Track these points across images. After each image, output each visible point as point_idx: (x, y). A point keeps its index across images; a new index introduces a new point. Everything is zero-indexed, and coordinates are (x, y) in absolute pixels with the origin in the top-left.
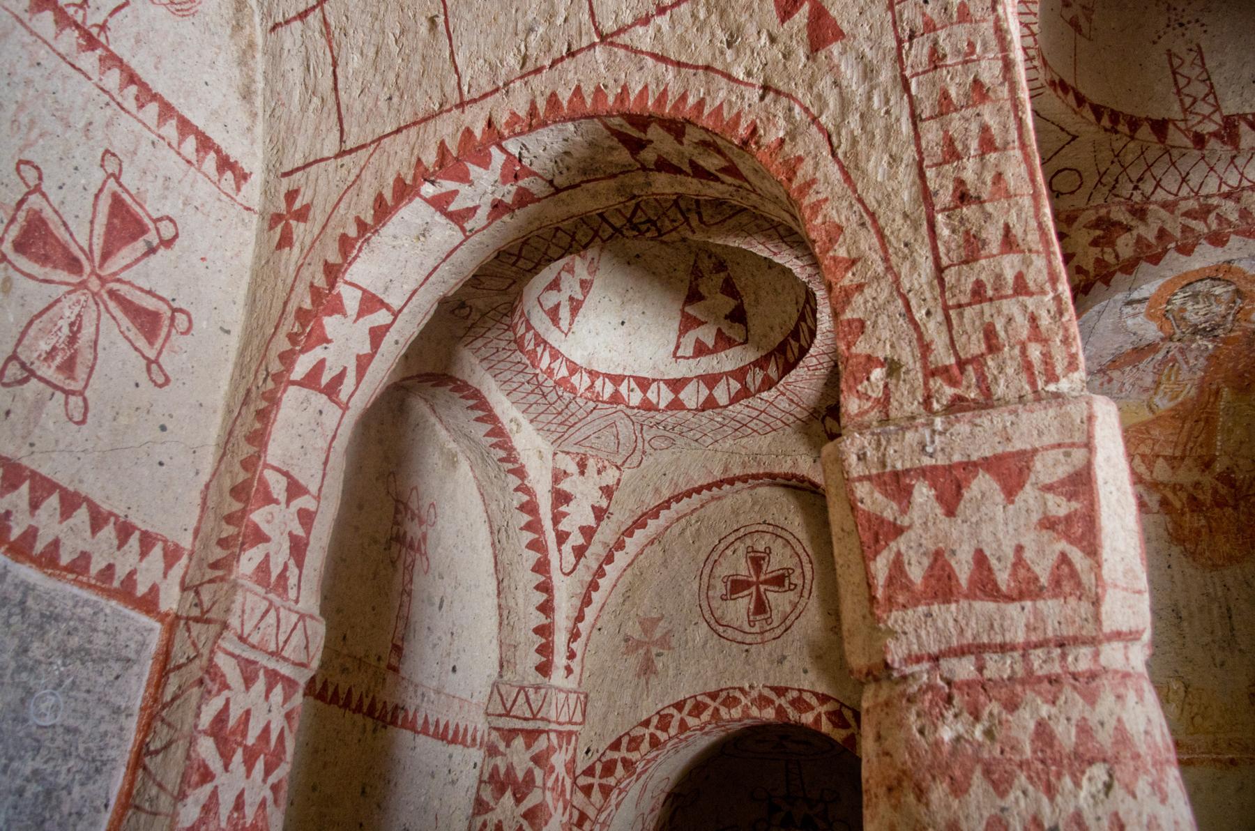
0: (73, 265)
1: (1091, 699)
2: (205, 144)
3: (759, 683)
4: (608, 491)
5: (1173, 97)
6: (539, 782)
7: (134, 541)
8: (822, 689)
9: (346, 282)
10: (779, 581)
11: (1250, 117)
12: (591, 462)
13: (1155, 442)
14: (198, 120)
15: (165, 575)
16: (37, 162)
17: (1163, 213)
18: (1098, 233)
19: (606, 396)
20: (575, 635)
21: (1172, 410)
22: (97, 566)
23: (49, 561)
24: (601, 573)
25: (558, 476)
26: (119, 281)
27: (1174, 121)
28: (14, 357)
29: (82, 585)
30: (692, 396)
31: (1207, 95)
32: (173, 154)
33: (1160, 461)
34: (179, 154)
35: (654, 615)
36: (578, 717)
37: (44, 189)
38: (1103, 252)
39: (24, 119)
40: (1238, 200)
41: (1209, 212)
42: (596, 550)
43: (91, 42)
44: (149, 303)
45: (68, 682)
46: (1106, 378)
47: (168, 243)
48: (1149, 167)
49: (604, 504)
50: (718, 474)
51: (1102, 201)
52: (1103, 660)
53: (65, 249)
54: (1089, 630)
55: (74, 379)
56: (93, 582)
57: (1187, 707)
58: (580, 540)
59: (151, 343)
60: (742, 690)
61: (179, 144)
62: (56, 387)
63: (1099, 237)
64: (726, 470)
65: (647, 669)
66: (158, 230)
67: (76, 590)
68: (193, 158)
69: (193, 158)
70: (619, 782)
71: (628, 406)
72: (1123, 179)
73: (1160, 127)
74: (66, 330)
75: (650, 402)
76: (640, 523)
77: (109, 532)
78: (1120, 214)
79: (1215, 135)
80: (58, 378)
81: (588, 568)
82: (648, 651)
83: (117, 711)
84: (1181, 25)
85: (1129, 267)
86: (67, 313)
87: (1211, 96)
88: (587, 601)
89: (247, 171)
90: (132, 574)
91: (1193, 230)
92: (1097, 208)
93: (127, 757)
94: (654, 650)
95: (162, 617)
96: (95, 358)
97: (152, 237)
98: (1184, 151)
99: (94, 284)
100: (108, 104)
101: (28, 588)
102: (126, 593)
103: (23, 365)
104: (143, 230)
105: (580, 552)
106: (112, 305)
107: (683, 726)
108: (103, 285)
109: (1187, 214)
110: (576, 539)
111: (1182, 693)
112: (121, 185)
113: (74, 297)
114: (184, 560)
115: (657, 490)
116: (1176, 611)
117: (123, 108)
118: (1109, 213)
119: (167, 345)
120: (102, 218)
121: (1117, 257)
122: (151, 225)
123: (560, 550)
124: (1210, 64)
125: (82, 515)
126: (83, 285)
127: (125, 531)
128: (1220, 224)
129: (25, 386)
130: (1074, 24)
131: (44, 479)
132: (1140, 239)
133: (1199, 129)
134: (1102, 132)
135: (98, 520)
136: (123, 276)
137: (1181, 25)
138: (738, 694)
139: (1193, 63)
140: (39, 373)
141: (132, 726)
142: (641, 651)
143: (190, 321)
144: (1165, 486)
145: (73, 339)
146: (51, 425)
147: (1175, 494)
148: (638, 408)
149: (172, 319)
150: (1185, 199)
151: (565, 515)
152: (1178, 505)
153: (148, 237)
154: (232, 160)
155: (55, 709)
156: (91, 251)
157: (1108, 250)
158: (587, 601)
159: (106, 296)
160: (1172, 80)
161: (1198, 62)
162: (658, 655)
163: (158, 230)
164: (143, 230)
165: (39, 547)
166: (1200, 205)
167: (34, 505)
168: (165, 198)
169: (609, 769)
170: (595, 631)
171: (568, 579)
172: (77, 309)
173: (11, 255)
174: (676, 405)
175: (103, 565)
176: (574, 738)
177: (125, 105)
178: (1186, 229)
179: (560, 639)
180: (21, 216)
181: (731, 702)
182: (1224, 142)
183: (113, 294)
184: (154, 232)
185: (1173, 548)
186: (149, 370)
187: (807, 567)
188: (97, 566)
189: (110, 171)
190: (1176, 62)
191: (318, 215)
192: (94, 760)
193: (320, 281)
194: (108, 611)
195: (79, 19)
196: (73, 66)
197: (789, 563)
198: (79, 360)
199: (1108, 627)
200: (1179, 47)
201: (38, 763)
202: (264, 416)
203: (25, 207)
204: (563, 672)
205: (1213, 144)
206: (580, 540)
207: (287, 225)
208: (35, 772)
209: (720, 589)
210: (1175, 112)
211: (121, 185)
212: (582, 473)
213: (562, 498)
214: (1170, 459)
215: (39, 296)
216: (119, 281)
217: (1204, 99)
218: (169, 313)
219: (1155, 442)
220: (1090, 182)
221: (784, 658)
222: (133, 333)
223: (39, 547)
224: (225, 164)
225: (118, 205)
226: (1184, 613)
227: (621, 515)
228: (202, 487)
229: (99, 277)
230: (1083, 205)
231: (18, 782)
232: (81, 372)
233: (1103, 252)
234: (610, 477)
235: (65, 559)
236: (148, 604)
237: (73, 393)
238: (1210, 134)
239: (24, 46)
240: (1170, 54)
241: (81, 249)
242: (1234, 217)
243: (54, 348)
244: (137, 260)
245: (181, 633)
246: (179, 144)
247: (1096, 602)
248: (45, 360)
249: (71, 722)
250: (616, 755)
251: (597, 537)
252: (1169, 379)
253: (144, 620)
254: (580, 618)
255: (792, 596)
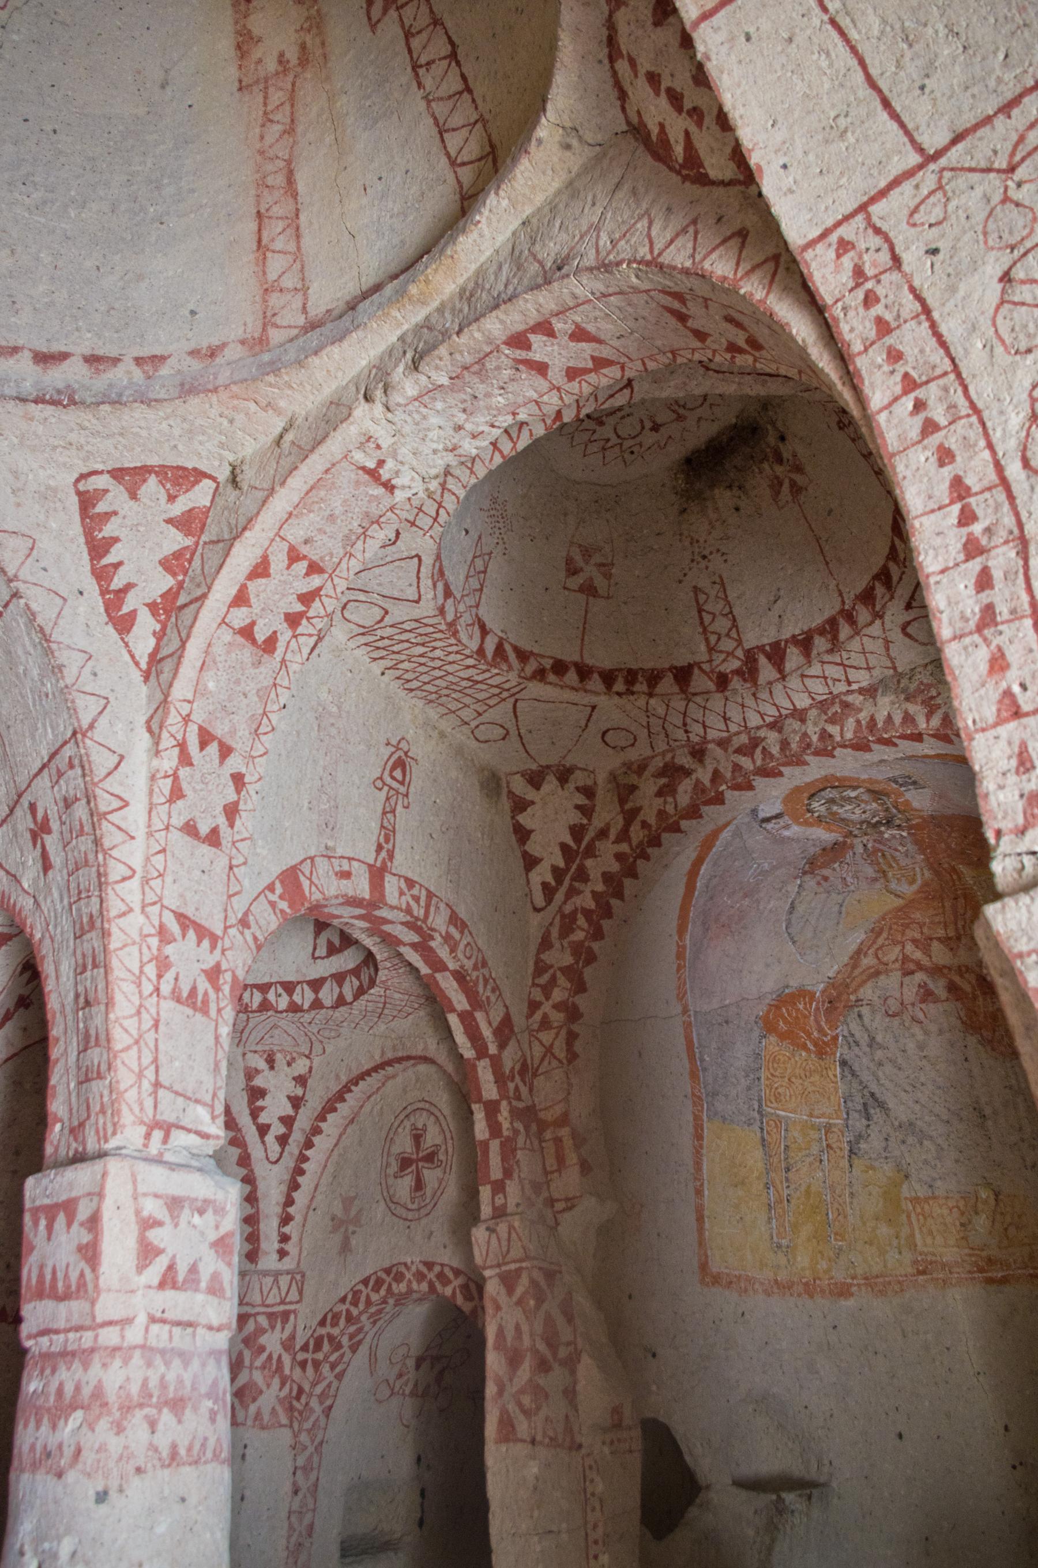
1: (86, 1365)
3: (414, 1259)
4: (301, 1080)
5: (699, 639)
6: (247, 1363)
8: (455, 1264)
10: (430, 1158)
11: (767, 648)
12: (279, 1056)
13: (921, 926)
17: (719, 751)
18: (663, 781)
19: (255, 1005)
20: (286, 1219)
21: (919, 891)
24: (303, 1158)
25: (250, 1074)
27: (698, 664)
30: (328, 994)
31: (730, 630)
33: (935, 944)
35: (353, 1194)
36: (294, 1295)
38: (665, 802)
40: (780, 731)
41: (756, 746)
42: (297, 1137)
46: (819, 878)
48: (685, 714)
49: (299, 1092)
50: (378, 1059)
51: (665, 747)
52: (100, 1339)
54: (88, 1323)
57: (998, 1217)
58: (282, 1130)
60: (405, 1264)
63: (664, 785)
64: (383, 1053)
65: (345, 1247)
70: (326, 1357)
71: (277, 1012)
72: (670, 728)
73: (683, 675)
75: (296, 1004)
76: (329, 1107)
78: (684, 760)
79: (738, 672)
81: (291, 1154)
82: (346, 1230)
84: (704, 557)
85: (693, 812)
87: (734, 630)
88: (294, 1186)
91: (741, 768)
92: (663, 754)
94: (351, 1228)
98: (706, 696)
105: (283, 1140)
107: (369, 1303)
109: (738, 751)
110: (278, 1129)
111: (992, 1202)
115: (337, 1077)
116: (978, 1109)
118: (673, 758)
121: (676, 806)
123: (263, 1142)
124: (732, 595)
128: (763, 759)
130: (589, 590)
132: (698, 782)
133: (722, 668)
134: (616, 697)
137: (704, 557)
138: (403, 1269)
139: (717, 597)
142: (343, 1230)
144: (950, 969)
147: (961, 976)
148: (286, 1011)
150: (738, 733)
151: (262, 1109)
152: (968, 988)
157: (670, 799)
158: (294, 1186)
160: (697, 621)
161: (721, 595)
162: (354, 1233)
166: (750, 739)
169: (318, 1346)
170: (311, 1212)
171: (276, 1168)
174: (317, 1004)
176: (292, 1317)
178: (737, 767)
179: (269, 1227)
181: (399, 1278)
182: (745, 680)
185: (969, 1038)
187: (450, 1145)
190: (702, 598)
197: (438, 1140)
199: (99, 1320)
200: (704, 583)
204: (275, 1256)
205: (736, 683)
206: (282, 1130)
209: (394, 1167)
210: (701, 653)
212: (272, 1068)
213: (256, 1094)
214: (945, 941)
217: (728, 635)
219: (921, 926)
220: (643, 734)
221: (431, 1233)
226: (988, 1111)
227: (314, 1103)
230: (649, 752)
233: (665, 802)
234: (301, 1067)
238: (732, 672)
240: (696, 590)
242: (775, 750)
247: (93, 1303)
250: (323, 1331)
251: (297, 1125)
252: (891, 866)
254: (289, 1202)
255: (438, 1172)
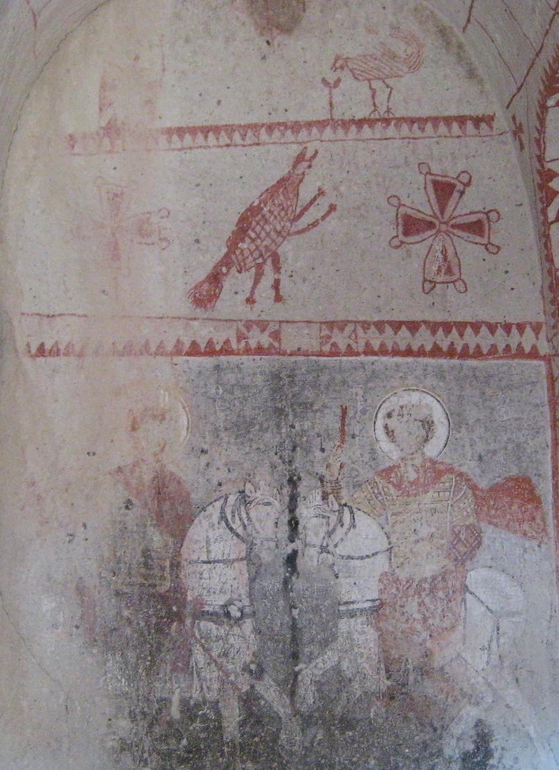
0: (431, 225)
2: (462, 120)
7: (514, 330)
9: (548, 162)
14: (453, 111)
15: (537, 339)
16: (394, 193)
22: (501, 347)
23: (478, 354)
26: (454, 218)
28: (425, 280)
29: (498, 358)
32: (449, 140)
34: (452, 137)
37: (403, 203)
39: (380, 180)
43: (387, 121)
44: (473, 218)
45: (507, 400)
47: (468, 184)
53: (423, 221)
55: (454, 274)
56: (502, 355)
59: (482, 236)
61: (450, 132)
62: (447, 283)
66: (459, 181)
67: (496, 362)
68: (460, 133)
69: (460, 133)
74: (441, 256)
77: (500, 331)
80: (448, 278)
83: (537, 405)
86: (437, 248)
89: (492, 114)
90: (519, 345)
93: (549, 423)
95: (544, 358)
96: (459, 260)
97: (460, 187)
99: (444, 227)
100: (409, 143)
101: (475, 369)
102: (520, 353)
103: (430, 282)
104: (452, 186)
106: (455, 231)
108: (448, 226)
112: (433, 175)
113: (437, 239)
114: (544, 328)
117: (416, 139)
119: (491, 231)
120: (432, 196)
122: (456, 182)
125: (484, 329)
126: (439, 231)
127: (507, 328)
129: (435, 289)
131: (459, 322)
135: (492, 328)
136: (456, 214)
140: (438, 281)
141: (547, 409)
143: (498, 213)
145: (445, 258)
146: (453, 299)
149: (488, 218)
153: (457, 188)
154: (480, 116)
155: (506, 412)
156: (435, 214)
159: (451, 230)
163: (459, 181)
164: (452, 186)
165: (471, 351)
167: (461, 335)
168: (456, 163)
172: (441, 244)
173: (405, 239)
175: (504, 346)
177: (416, 136)
180: (400, 220)
183: (453, 226)
184: (459, 184)
186: (487, 249)
188: (501, 347)
189: (425, 172)
191: (525, 128)
192: (533, 428)
193: (537, 165)
194: (515, 365)
195: (377, 117)
196: (386, 139)
198: (452, 265)
201: (509, 435)
202: (546, 245)
203: (399, 216)
207: (519, 136)
208: (509, 439)
211: (433, 175)
215: (421, 249)
216: (454, 218)
218: (485, 216)
222: (473, 237)
223: (471, 351)
224: (477, 121)
225: (436, 184)
228: (540, 289)
229: (444, 223)
231: (503, 445)
232: (455, 270)
235: (485, 351)
236: (534, 354)
237: (456, 281)
239: (364, 149)
241: (431, 216)
243: (439, 267)
244: (458, 203)
245: (553, 363)
246: (450, 132)
248: (438, 274)
249: (516, 416)
253: (535, 362)
